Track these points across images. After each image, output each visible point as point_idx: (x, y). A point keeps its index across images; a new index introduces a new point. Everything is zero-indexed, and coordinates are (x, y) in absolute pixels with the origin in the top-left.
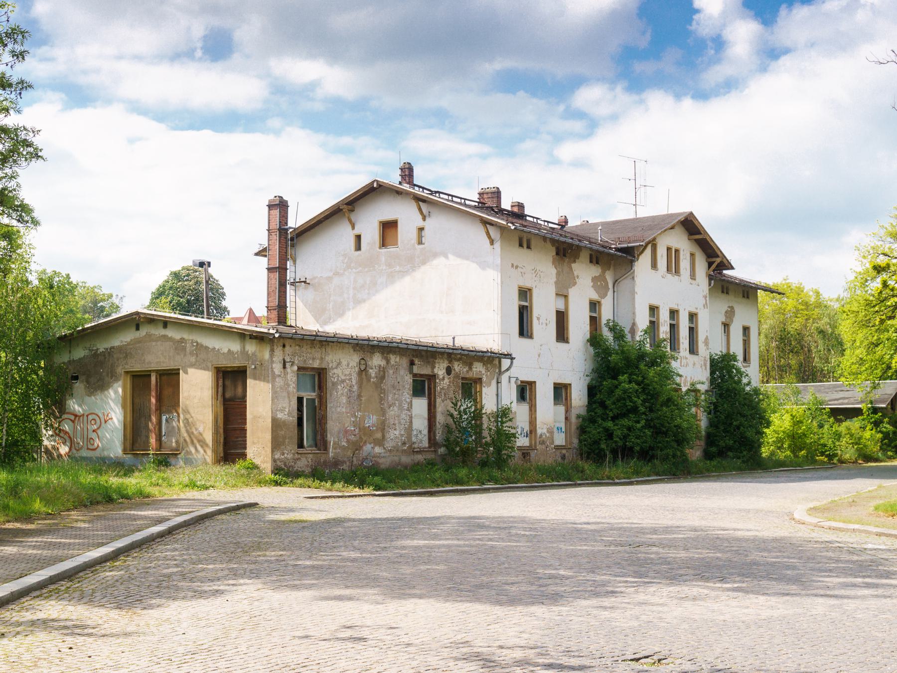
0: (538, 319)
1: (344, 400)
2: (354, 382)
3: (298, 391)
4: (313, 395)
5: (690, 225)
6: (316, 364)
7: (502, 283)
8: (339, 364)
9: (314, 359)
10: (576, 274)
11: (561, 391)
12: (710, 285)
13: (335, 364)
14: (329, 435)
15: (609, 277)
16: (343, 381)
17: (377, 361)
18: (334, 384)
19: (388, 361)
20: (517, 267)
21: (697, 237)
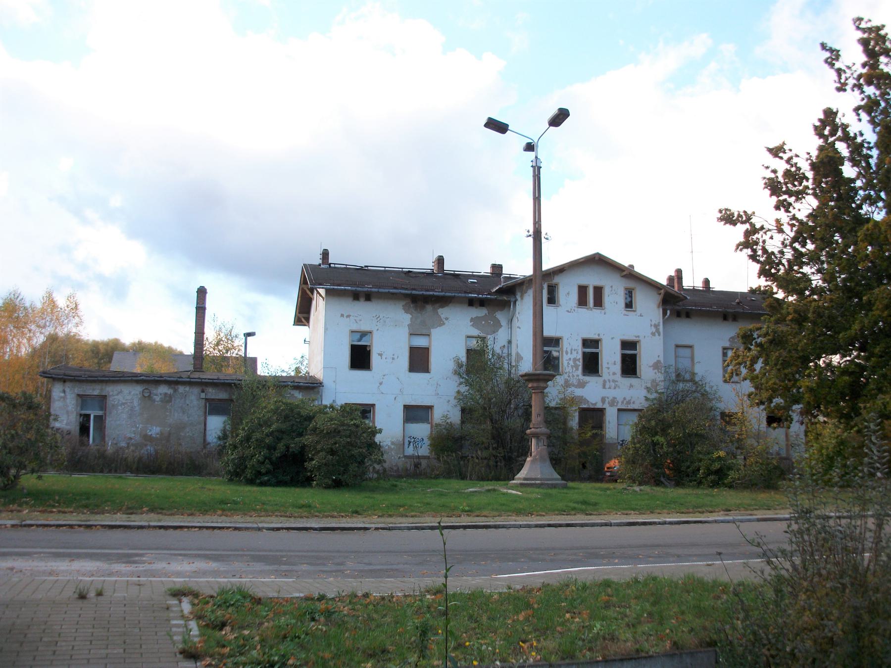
0: (380, 355)
1: (124, 416)
2: (136, 403)
3: (82, 409)
4: (100, 413)
5: (597, 261)
6: (96, 393)
7: (326, 329)
8: (121, 392)
9: (94, 390)
10: (443, 316)
11: (415, 413)
12: (664, 313)
13: (115, 393)
14: (107, 439)
15: (501, 316)
16: (124, 404)
17: (163, 389)
18: (113, 405)
19: (175, 391)
20: (348, 316)
21: (625, 273)
